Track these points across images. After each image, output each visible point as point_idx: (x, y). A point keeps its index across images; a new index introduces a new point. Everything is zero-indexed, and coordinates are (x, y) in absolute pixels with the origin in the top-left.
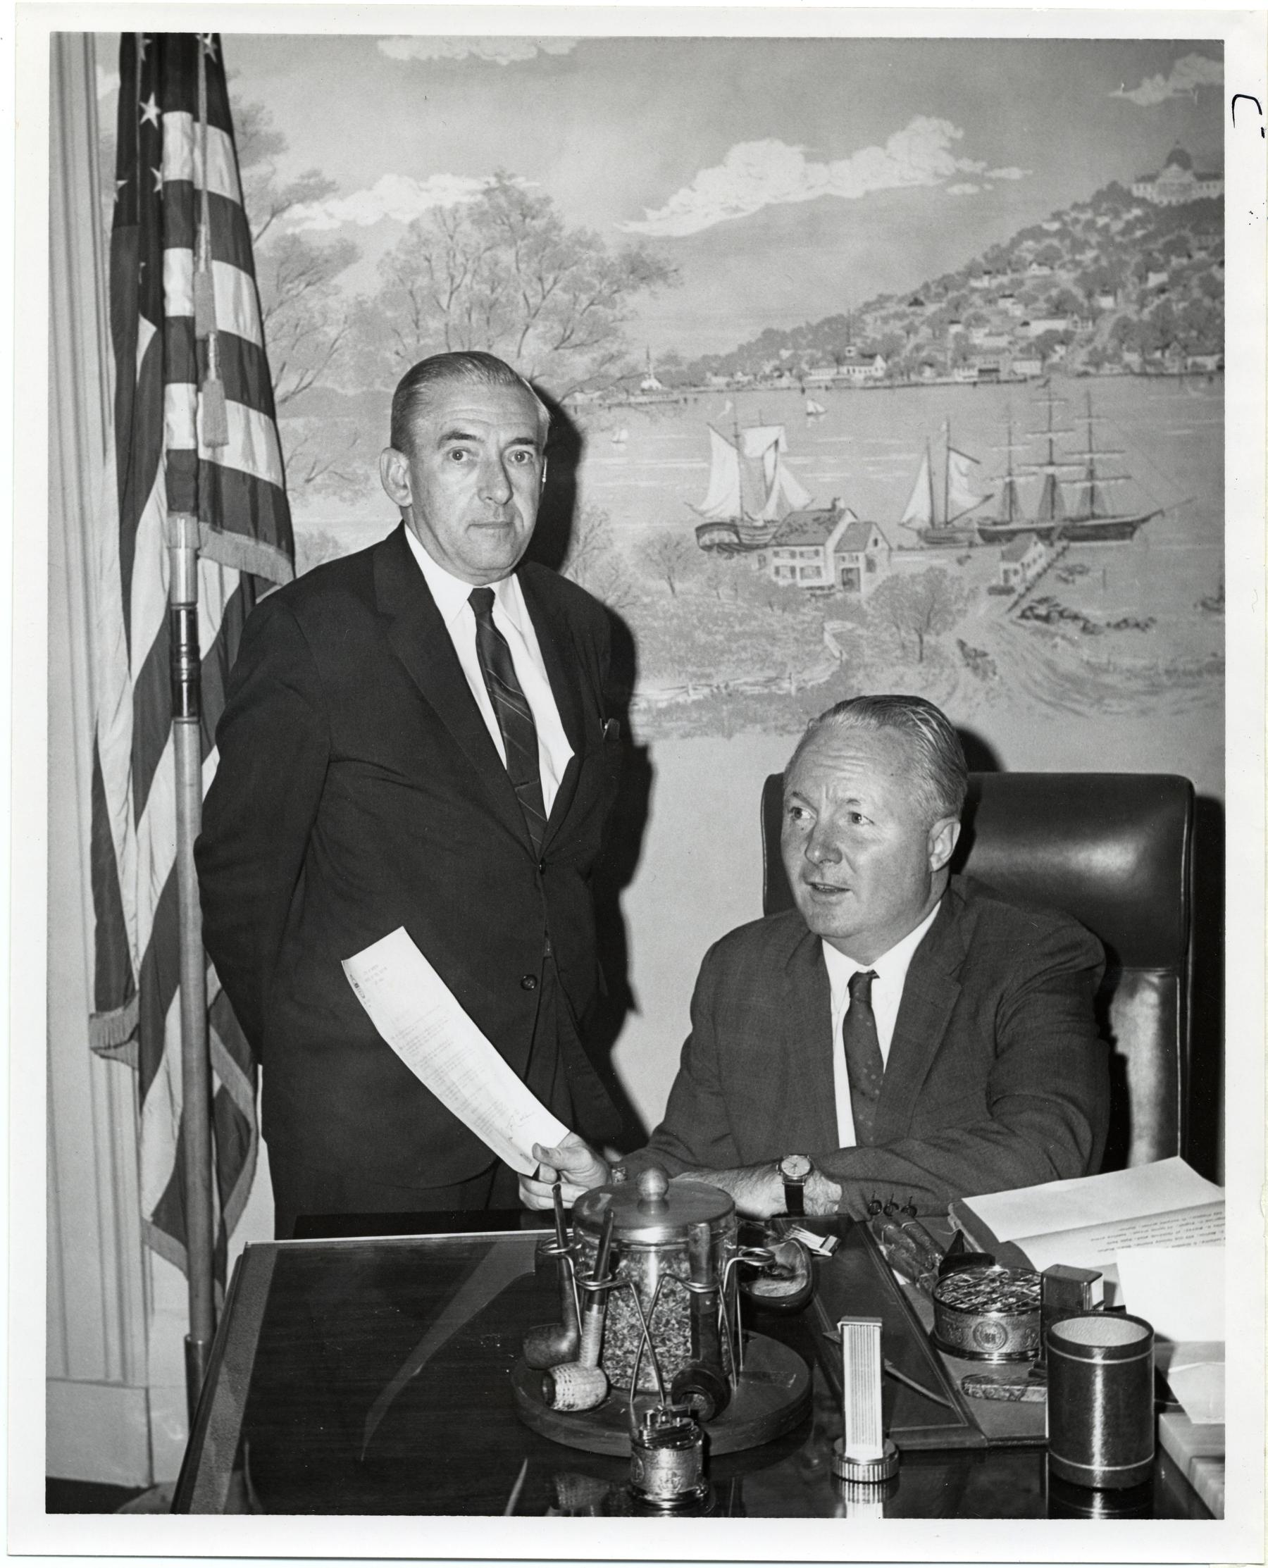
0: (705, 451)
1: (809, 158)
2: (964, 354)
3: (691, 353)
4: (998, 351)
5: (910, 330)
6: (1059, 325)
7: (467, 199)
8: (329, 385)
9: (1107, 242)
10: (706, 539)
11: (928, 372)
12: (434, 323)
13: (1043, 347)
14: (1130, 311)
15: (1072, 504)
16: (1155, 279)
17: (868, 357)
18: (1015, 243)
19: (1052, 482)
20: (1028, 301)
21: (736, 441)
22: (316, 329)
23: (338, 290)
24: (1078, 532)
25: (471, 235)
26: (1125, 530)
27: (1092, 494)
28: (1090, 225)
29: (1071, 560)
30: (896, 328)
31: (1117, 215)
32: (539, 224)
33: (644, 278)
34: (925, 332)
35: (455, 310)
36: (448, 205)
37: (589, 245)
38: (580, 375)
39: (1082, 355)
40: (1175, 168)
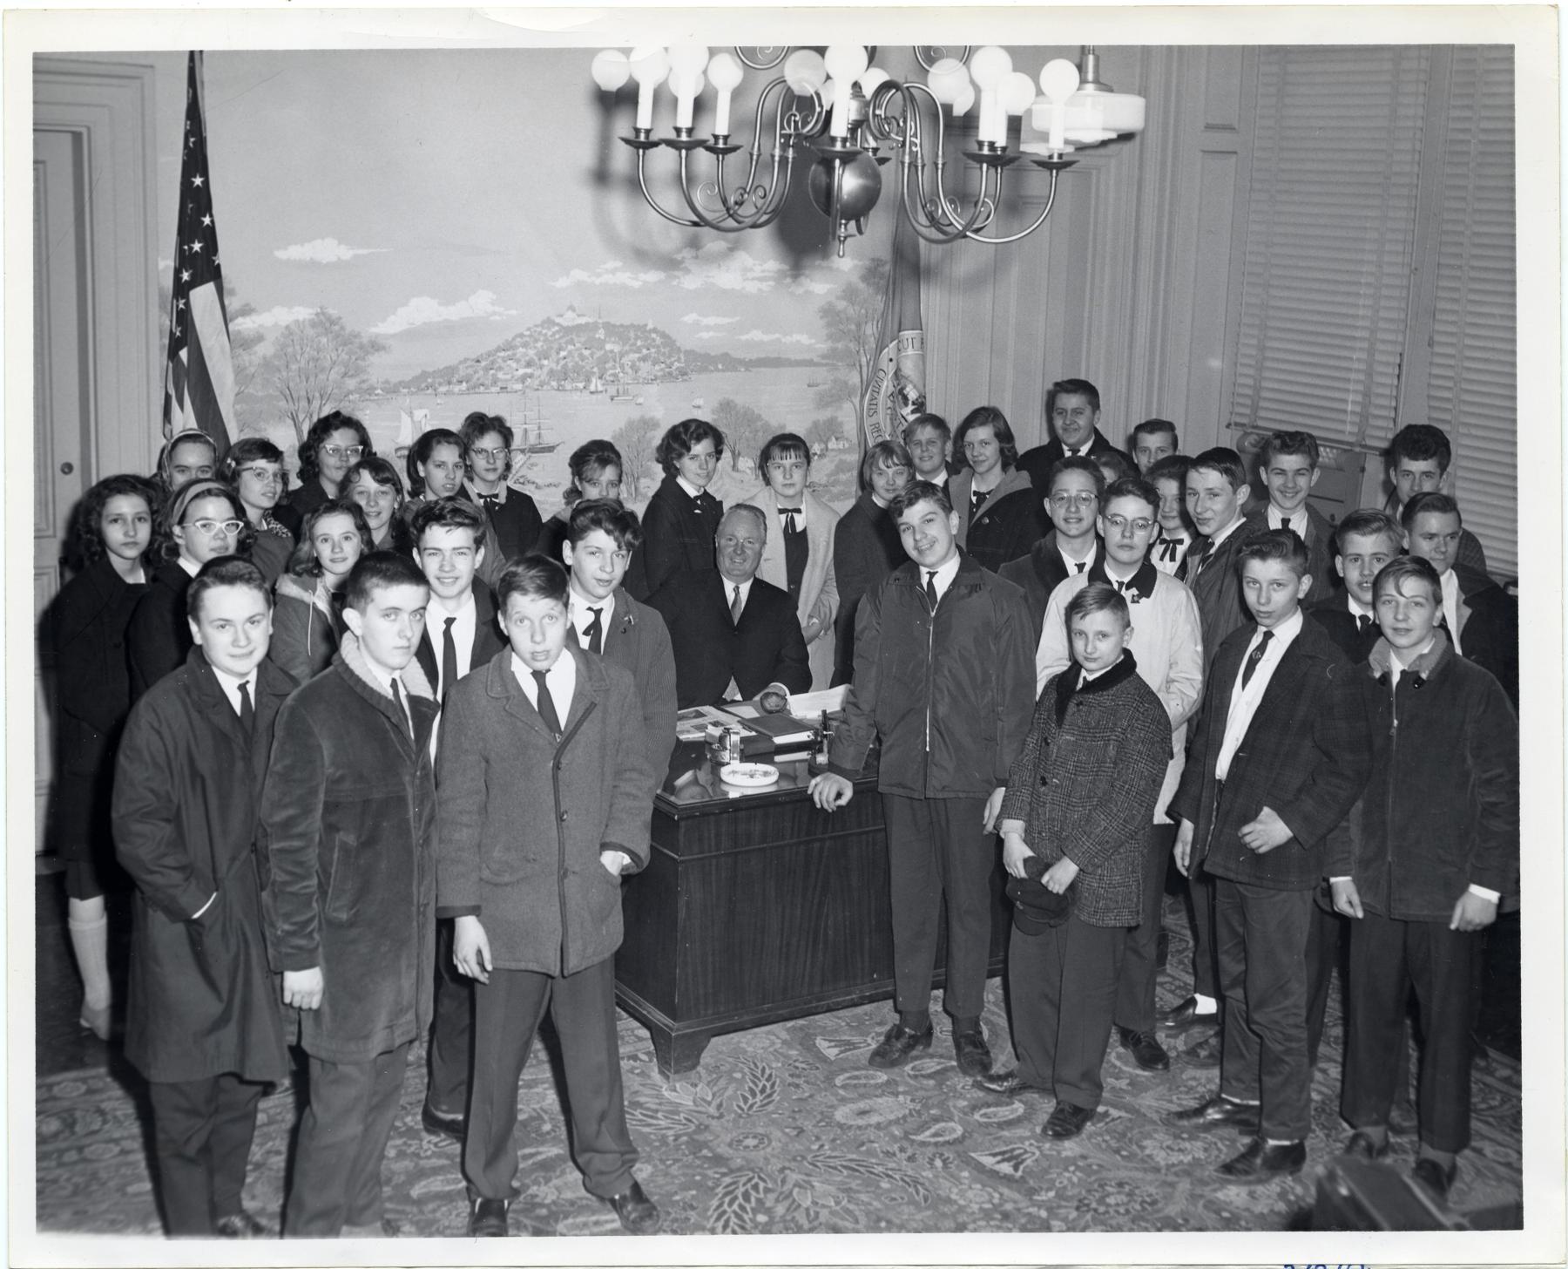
0: (399, 418)
1: (440, 304)
2: (495, 383)
3: (394, 380)
4: (506, 380)
5: (475, 372)
6: (529, 371)
7: (307, 317)
8: (251, 391)
9: (546, 340)
10: (399, 453)
11: (482, 388)
12: (294, 367)
13: (523, 379)
14: (554, 366)
15: (532, 440)
16: (563, 354)
17: (460, 382)
18: (514, 339)
19: (526, 431)
20: (518, 361)
21: (411, 414)
22: (245, 368)
23: (255, 353)
24: (534, 450)
25: (310, 332)
26: (551, 449)
27: (539, 436)
28: (540, 333)
29: (532, 461)
30: (470, 371)
31: (549, 329)
32: (337, 328)
33: (377, 350)
34: (481, 373)
35: (303, 362)
36: (301, 318)
37: (355, 336)
38: (352, 387)
39: (537, 382)
40: (570, 312)
